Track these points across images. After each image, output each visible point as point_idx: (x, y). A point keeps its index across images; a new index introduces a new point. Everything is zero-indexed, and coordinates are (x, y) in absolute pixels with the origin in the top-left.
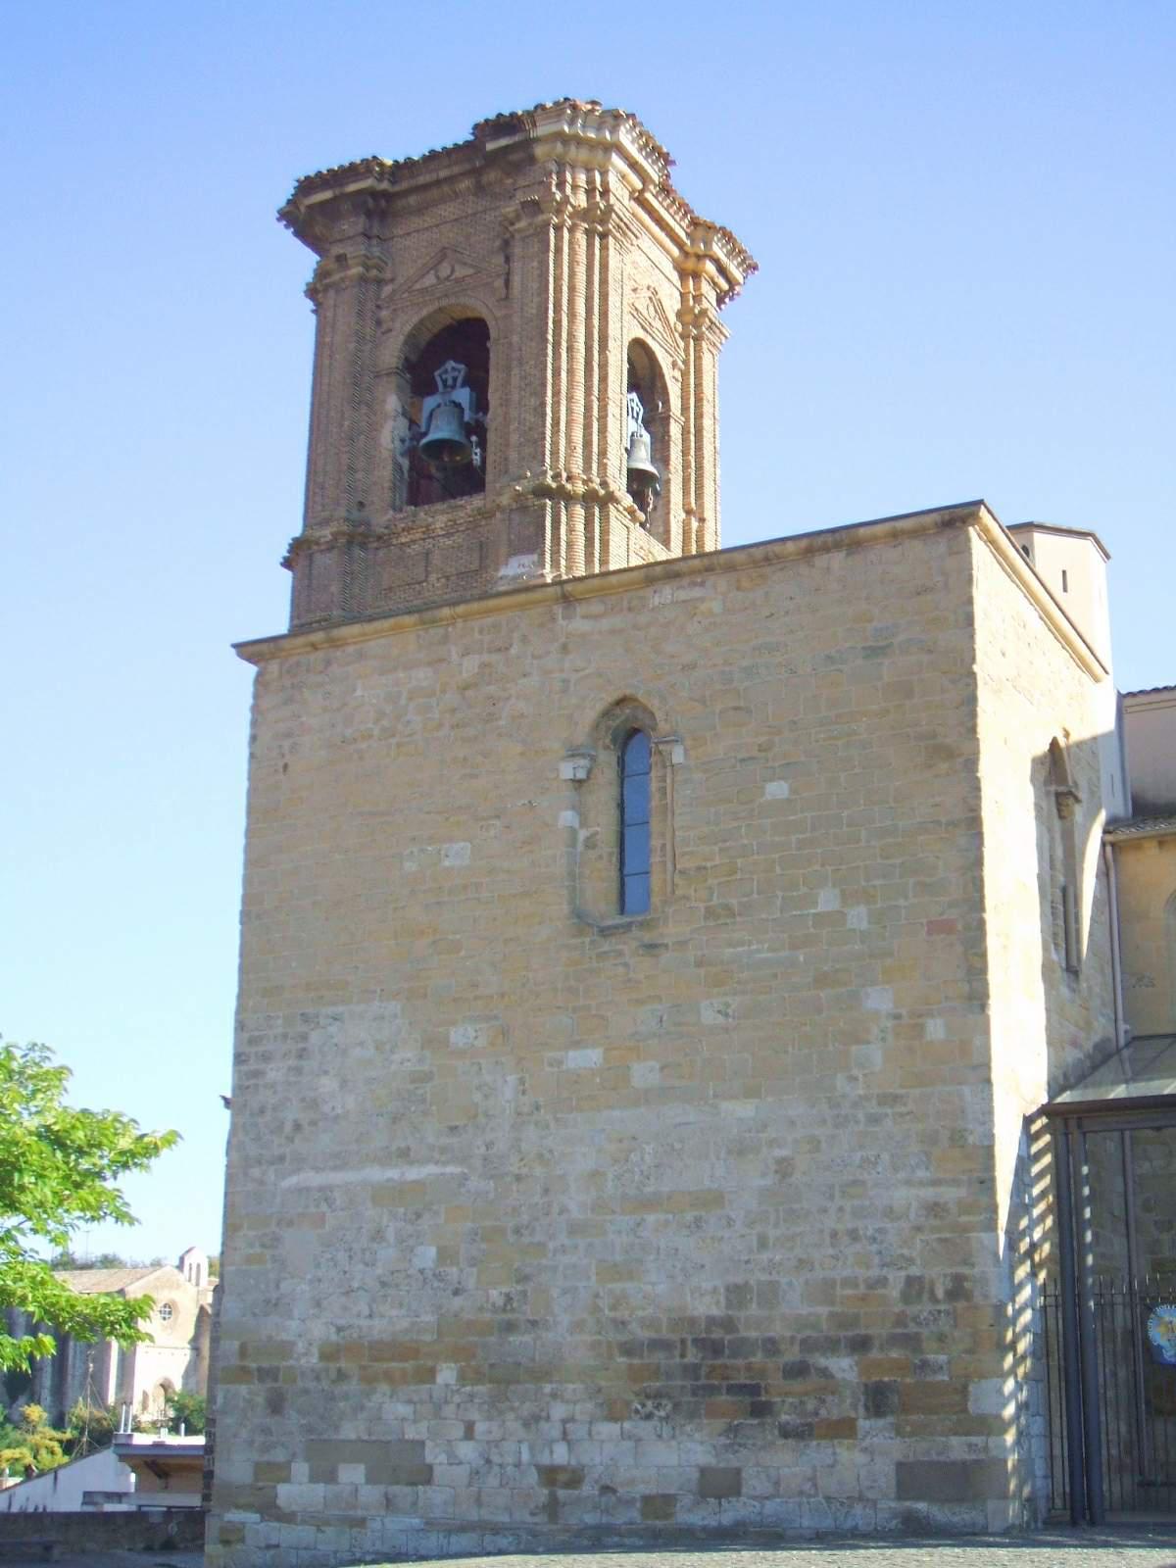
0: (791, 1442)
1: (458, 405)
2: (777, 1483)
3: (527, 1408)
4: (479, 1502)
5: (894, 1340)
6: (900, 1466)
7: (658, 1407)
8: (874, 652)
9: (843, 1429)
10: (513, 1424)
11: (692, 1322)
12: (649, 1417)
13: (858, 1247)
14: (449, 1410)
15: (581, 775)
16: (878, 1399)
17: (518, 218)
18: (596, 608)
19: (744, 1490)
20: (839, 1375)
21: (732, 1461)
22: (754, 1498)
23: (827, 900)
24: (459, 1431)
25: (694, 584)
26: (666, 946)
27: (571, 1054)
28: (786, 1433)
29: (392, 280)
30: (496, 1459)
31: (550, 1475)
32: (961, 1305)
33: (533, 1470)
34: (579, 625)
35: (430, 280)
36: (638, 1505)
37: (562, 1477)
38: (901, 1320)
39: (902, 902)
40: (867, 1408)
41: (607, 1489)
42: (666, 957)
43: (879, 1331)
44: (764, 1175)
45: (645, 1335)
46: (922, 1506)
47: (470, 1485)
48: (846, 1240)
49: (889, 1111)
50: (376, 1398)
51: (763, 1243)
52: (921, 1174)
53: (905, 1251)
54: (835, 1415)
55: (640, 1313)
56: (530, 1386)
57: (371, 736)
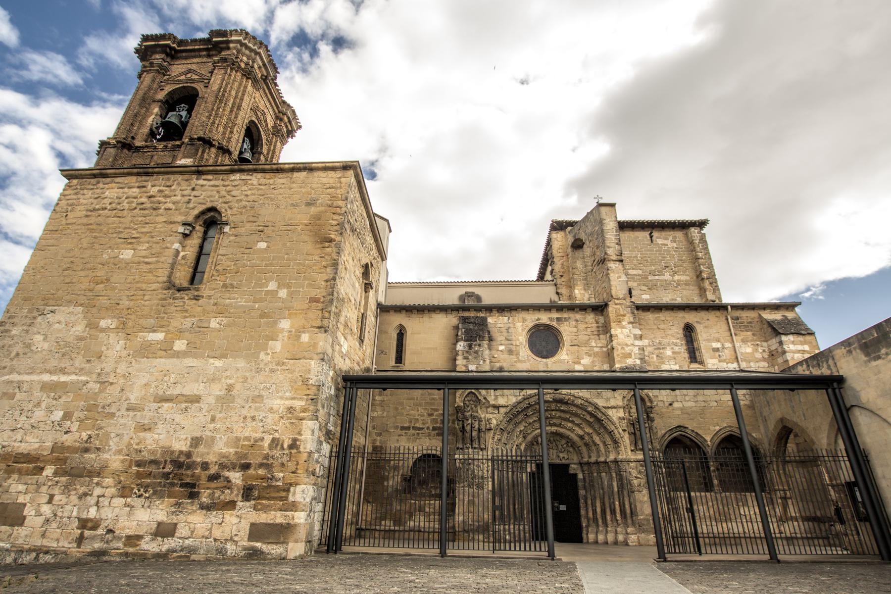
0: (204, 512)
1: (181, 116)
2: (192, 532)
3: (82, 490)
4: (43, 536)
5: (261, 465)
6: (253, 525)
7: (145, 492)
8: (308, 204)
9: (231, 505)
10: (74, 498)
11: (173, 452)
12: (140, 496)
13: (254, 423)
14: (44, 489)
15: (187, 232)
16: (247, 493)
17: (218, 62)
18: (210, 177)
19: (176, 534)
20: (233, 481)
21: (174, 519)
22: (180, 538)
23: (272, 286)
24: (46, 499)
25: (248, 174)
26: (203, 297)
27: (151, 334)
28: (202, 507)
29: (169, 75)
30: (60, 514)
31: (84, 524)
32: (294, 451)
33: (77, 519)
34: (201, 182)
35: (183, 77)
36: (123, 540)
37: (90, 525)
38: (267, 457)
39: (301, 290)
40: (243, 497)
41: (110, 531)
42: (201, 302)
43: (255, 460)
44: (220, 390)
45: (147, 456)
46: (258, 545)
47: (42, 527)
48: (249, 420)
49: (279, 368)
50: (10, 481)
51: (213, 420)
52: (287, 394)
53: (275, 427)
54: (228, 499)
55: (149, 447)
56: (87, 479)
57: (106, 208)
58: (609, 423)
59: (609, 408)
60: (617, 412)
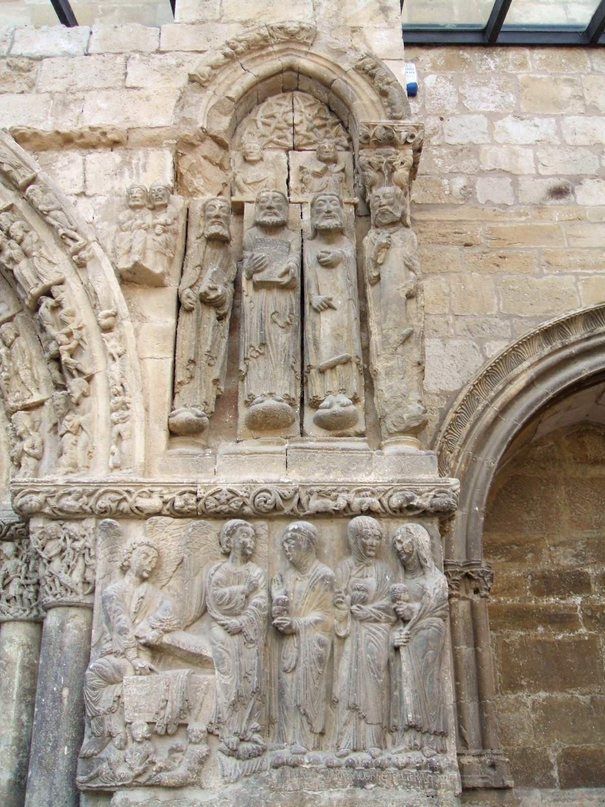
58: (39, 231)
59: (67, 141)
60: (118, 172)
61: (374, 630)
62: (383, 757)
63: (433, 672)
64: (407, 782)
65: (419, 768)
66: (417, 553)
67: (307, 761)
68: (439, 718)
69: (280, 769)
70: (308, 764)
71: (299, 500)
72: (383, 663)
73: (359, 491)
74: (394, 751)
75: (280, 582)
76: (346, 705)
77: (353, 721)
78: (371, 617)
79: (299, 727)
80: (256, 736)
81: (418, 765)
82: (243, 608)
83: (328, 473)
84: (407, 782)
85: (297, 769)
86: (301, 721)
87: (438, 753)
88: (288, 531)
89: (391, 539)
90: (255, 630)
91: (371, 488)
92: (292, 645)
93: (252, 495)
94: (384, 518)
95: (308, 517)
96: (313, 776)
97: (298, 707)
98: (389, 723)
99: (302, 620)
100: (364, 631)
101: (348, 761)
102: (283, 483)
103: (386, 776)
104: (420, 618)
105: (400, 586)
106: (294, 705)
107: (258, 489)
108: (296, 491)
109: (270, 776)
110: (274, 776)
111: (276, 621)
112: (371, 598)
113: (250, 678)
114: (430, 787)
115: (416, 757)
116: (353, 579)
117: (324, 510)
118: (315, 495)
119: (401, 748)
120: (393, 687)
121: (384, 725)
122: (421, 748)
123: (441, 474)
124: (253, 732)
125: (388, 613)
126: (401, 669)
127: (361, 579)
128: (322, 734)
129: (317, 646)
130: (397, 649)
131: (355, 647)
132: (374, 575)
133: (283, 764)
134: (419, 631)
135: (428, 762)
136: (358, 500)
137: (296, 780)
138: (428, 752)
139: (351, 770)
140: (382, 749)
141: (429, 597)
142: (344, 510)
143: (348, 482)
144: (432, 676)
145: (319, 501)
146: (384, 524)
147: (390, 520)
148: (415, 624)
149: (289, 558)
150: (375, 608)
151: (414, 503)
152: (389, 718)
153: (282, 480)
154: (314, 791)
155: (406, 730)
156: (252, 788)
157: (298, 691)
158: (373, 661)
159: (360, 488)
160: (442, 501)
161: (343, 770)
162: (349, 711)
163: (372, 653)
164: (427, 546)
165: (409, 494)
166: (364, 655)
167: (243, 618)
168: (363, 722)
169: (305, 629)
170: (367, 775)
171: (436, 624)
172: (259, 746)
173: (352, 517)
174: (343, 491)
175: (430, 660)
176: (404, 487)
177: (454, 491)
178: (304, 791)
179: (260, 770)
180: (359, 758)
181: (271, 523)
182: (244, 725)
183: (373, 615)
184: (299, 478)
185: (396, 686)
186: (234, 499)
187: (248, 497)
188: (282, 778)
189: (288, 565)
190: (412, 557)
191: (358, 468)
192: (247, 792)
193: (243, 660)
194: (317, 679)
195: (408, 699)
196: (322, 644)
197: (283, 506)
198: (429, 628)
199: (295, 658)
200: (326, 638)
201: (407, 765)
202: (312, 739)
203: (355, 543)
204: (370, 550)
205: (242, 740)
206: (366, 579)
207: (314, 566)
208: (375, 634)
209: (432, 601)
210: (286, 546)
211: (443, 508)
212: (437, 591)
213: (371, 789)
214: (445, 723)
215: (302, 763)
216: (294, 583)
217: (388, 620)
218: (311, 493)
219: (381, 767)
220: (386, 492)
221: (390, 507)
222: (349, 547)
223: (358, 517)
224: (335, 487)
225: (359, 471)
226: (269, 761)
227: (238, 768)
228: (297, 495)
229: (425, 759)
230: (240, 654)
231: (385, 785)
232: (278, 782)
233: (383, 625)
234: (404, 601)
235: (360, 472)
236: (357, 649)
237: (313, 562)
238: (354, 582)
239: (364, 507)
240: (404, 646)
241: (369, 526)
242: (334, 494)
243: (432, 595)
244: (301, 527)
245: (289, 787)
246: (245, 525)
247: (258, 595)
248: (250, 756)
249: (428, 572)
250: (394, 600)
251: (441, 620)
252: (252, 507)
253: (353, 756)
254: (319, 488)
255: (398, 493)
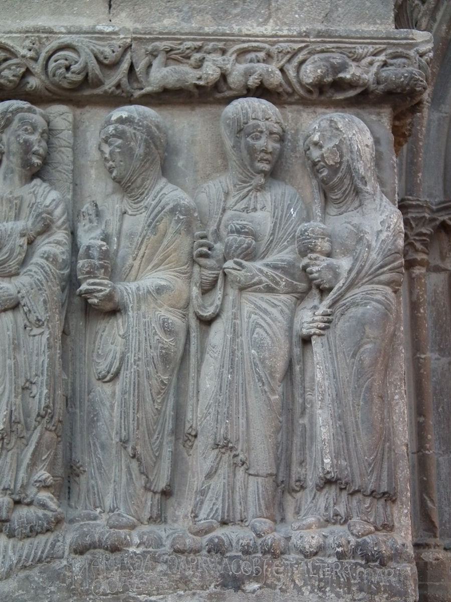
61: (264, 305)
62: (277, 535)
63: (372, 384)
64: (320, 580)
65: (341, 556)
66: (349, 166)
67: (137, 540)
68: (382, 468)
69: (88, 556)
70: (138, 546)
71: (132, 68)
72: (280, 365)
73: (243, 52)
74: (295, 526)
75: (93, 217)
76: (211, 441)
77: (224, 470)
78: (260, 282)
79: (124, 480)
80: (44, 495)
81: (340, 550)
82: (23, 263)
83: (188, 20)
84: (320, 580)
85: (118, 555)
86: (128, 468)
87: (377, 529)
88: (108, 123)
89: (301, 143)
90: (45, 302)
91: (267, 46)
92: (115, 330)
93: (43, 55)
94: (291, 104)
95: (150, 100)
96: (147, 569)
97: (124, 442)
98: (290, 476)
99: (132, 286)
100: (247, 308)
101: (211, 540)
102: (102, 33)
103: (281, 569)
104: (351, 286)
105: (316, 225)
106: (116, 440)
107: (54, 44)
108: (127, 48)
109: (69, 567)
110: (76, 568)
111: (84, 287)
112: (262, 249)
113: (35, 389)
114: (361, 590)
115: (339, 535)
116: (229, 213)
117: (178, 85)
118: (161, 58)
119: (311, 519)
120: (298, 410)
121: (280, 479)
122: (346, 521)
123: (400, 22)
124: (39, 489)
125: (292, 276)
126: (313, 379)
127: (244, 214)
128: (166, 493)
129: (161, 334)
130: (306, 341)
131: (229, 336)
132: (269, 207)
133: (93, 546)
134: (348, 308)
135: (358, 545)
136: (241, 67)
137: (116, 576)
138: (358, 528)
139: (217, 558)
140: (275, 521)
141: (369, 246)
142: (216, 87)
143: (224, 34)
144: (369, 389)
145: (168, 69)
146: (290, 115)
147: (301, 108)
148: (341, 296)
149: (111, 172)
150: (267, 265)
151: (347, 75)
152: (288, 466)
153: (99, 27)
154: (150, 595)
155: (320, 488)
156: (36, 589)
157: (124, 415)
158: (263, 361)
159: (246, 45)
160: (398, 73)
161: (202, 558)
162: (216, 451)
163: (260, 347)
164: (368, 153)
165: (337, 59)
166: (246, 351)
167: (23, 280)
168: (240, 472)
169: (139, 302)
170: (246, 567)
171: (379, 297)
172: (50, 514)
173: (228, 101)
174: (214, 50)
175: (367, 362)
176: (328, 46)
177: (421, 55)
178: (131, 594)
179: (52, 557)
180: (234, 537)
181: (78, 111)
182: (22, 474)
183: (264, 279)
184: (130, 25)
185: (304, 409)
186: (9, 62)
187: (35, 60)
188: (91, 571)
189: (111, 185)
190: (340, 175)
191: (243, 9)
192: (26, 597)
193: (21, 357)
194: (159, 393)
195: (324, 431)
196: (167, 329)
197: (101, 76)
198: (366, 304)
199: (118, 356)
200: (175, 319)
201: (320, 550)
202: (150, 501)
203: (234, 147)
204: (261, 160)
205: (17, 503)
206: (253, 214)
207: (158, 188)
208: (266, 312)
209: (374, 255)
210: (107, 149)
211: (401, 85)
212: (383, 236)
213: (254, 591)
214: (392, 476)
215: (129, 544)
216: (121, 220)
217: (292, 290)
218: (153, 54)
219: (273, 553)
220: (295, 53)
221: (300, 82)
222: (224, 156)
223: (240, 100)
224: (199, 43)
225: (245, 16)
226: (68, 541)
227: (10, 553)
228: (128, 56)
229: (353, 540)
230: (16, 347)
231: (280, 585)
232: (84, 578)
233: (283, 297)
234: (321, 252)
235: (248, 18)
236: (233, 340)
237: (156, 183)
238: (231, 219)
239: (253, 81)
240: (320, 335)
241: (260, 115)
242: (198, 56)
243: (374, 244)
244: (135, 115)
245: (104, 587)
246: (29, 110)
247: (51, 239)
248: (33, 532)
249: (369, 205)
250: (303, 253)
251: (389, 290)
252: (43, 77)
253: (221, 533)
254: (167, 44)
255: (316, 57)
